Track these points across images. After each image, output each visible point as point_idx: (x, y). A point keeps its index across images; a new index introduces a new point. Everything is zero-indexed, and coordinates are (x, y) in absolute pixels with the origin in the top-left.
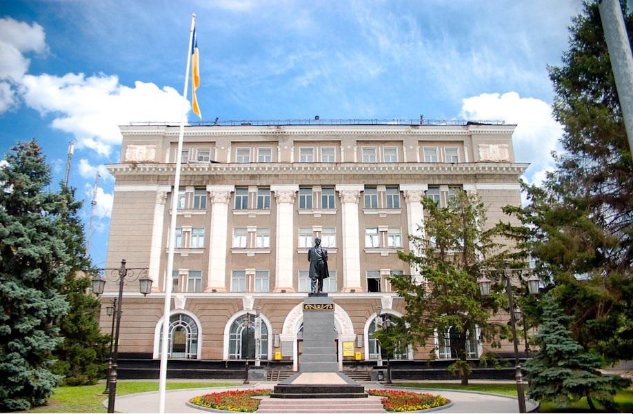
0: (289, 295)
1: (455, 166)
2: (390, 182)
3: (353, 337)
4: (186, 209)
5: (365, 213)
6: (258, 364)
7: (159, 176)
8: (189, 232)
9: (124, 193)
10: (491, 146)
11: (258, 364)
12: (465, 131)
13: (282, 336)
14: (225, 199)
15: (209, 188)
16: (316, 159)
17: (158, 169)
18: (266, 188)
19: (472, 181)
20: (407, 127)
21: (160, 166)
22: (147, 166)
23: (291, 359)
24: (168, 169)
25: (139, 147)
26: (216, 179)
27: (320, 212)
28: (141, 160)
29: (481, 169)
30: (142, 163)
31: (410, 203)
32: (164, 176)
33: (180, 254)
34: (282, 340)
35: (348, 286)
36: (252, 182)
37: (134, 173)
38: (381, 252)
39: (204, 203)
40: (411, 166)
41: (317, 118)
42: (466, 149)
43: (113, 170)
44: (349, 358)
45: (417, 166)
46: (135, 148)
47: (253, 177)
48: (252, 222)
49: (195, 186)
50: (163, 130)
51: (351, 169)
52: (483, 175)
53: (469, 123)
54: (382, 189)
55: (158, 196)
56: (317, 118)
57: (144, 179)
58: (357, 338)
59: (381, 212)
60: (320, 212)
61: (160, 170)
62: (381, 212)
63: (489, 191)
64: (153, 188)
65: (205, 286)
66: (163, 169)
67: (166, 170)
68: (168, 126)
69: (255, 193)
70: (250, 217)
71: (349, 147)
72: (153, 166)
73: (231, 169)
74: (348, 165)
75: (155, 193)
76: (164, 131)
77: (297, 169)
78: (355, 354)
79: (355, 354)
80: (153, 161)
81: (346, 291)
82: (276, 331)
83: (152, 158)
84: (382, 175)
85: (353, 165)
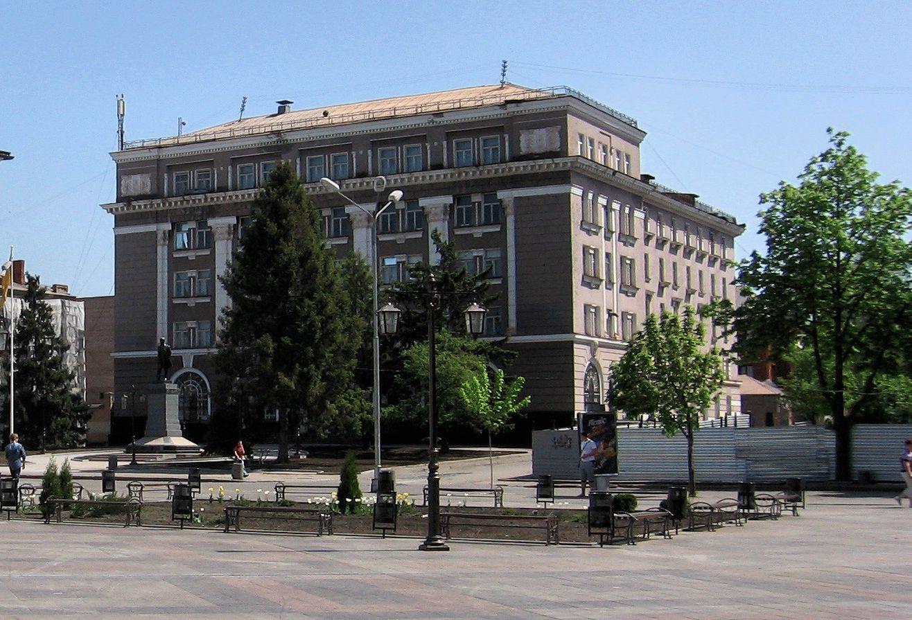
1: (481, 168)
4: (189, 249)
8: (194, 278)
10: (535, 131)
12: (505, 112)
14: (227, 236)
20: (429, 116)
21: (154, 202)
22: (142, 203)
24: (164, 205)
26: (213, 211)
32: (163, 211)
33: (186, 304)
37: (131, 211)
39: (208, 241)
40: (435, 173)
41: (325, 114)
50: (155, 153)
53: (507, 102)
55: (160, 236)
56: (325, 114)
57: (141, 218)
63: (528, 198)
64: (152, 228)
66: (158, 205)
67: (161, 205)
68: (160, 147)
72: (147, 202)
75: (155, 234)
76: (156, 153)
83: (148, 190)
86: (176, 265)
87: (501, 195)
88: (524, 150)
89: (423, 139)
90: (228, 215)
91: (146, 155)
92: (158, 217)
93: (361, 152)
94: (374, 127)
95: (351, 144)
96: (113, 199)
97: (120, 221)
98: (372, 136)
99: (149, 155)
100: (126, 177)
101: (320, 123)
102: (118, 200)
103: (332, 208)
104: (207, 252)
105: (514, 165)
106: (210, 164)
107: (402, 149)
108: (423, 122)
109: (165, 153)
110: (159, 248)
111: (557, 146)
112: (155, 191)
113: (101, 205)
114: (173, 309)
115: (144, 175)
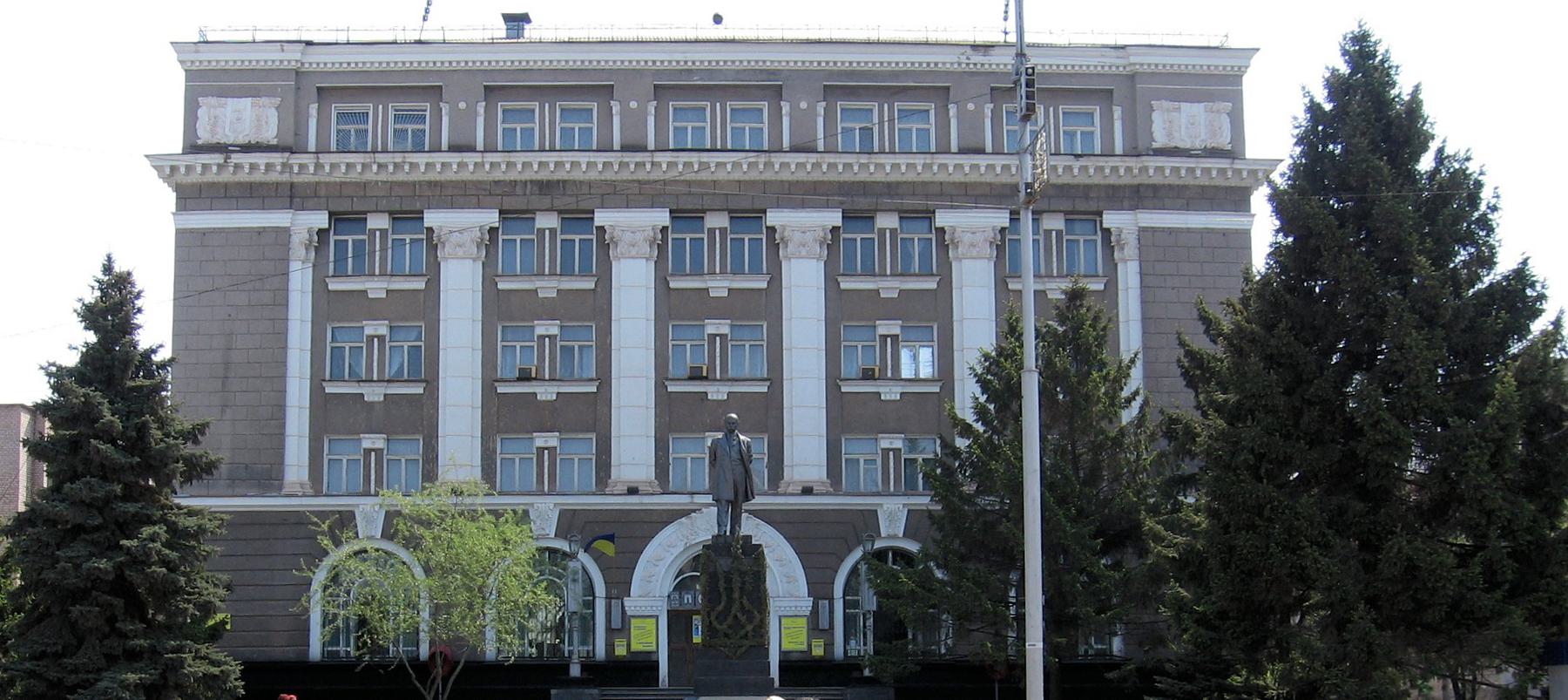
0: (646, 500)
2: (910, 202)
3: (807, 604)
5: (843, 286)
6: (575, 671)
7: (292, 185)
8: (381, 338)
9: (204, 233)
10: (1184, 106)
11: (575, 671)
13: (627, 602)
15: (432, 218)
16: (713, 138)
17: (291, 167)
18: (577, 218)
19: (1126, 203)
20: (962, 50)
21: (296, 160)
22: (261, 159)
23: (654, 658)
25: (232, 104)
27: (727, 284)
28: (242, 140)
29: (1151, 172)
30: (247, 148)
31: (960, 260)
32: (308, 184)
34: (629, 613)
35: (797, 477)
36: (546, 202)
38: (881, 390)
42: (1117, 112)
43: (168, 171)
44: (794, 657)
45: (982, 161)
46: (223, 106)
47: (545, 187)
48: (548, 310)
49: (391, 213)
50: (293, 56)
51: (809, 167)
52: (1155, 188)
54: (887, 221)
55: (299, 238)
58: (815, 606)
59: (887, 284)
60: (727, 284)
61: (296, 169)
62: (887, 284)
65: (430, 474)
68: (309, 43)
69: (553, 231)
70: (540, 295)
71: (803, 105)
72: (277, 159)
73: (487, 167)
74: (801, 158)
75: (283, 234)
76: (298, 56)
77: (664, 166)
78: (810, 646)
79: (810, 646)
80: (275, 142)
81: (790, 490)
82: (614, 592)
83: (270, 134)
84: (889, 185)
85: (813, 158)
86: (328, 306)
87: (1111, 219)
88: (1160, 141)
89: (941, 94)
90: (479, 206)
91: (273, 57)
92: (293, 196)
93: (803, 105)
94: (839, 58)
95: (781, 86)
96: (176, 146)
97: (190, 197)
98: (831, 74)
99: (278, 56)
100: (213, 101)
101: (702, 35)
102: (192, 148)
103: (730, 211)
104: (420, 284)
105: (1153, 162)
106: (435, 93)
107: (891, 110)
108: (947, 60)
109: (315, 59)
110: (295, 266)
111: (1224, 141)
112: (289, 140)
113: (147, 156)
114: (322, 404)
115: (264, 100)
